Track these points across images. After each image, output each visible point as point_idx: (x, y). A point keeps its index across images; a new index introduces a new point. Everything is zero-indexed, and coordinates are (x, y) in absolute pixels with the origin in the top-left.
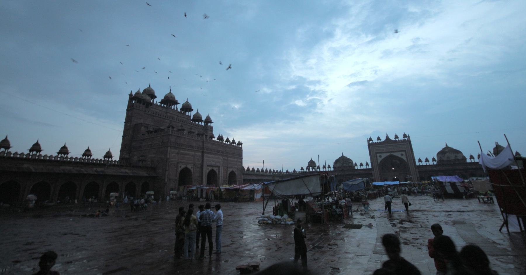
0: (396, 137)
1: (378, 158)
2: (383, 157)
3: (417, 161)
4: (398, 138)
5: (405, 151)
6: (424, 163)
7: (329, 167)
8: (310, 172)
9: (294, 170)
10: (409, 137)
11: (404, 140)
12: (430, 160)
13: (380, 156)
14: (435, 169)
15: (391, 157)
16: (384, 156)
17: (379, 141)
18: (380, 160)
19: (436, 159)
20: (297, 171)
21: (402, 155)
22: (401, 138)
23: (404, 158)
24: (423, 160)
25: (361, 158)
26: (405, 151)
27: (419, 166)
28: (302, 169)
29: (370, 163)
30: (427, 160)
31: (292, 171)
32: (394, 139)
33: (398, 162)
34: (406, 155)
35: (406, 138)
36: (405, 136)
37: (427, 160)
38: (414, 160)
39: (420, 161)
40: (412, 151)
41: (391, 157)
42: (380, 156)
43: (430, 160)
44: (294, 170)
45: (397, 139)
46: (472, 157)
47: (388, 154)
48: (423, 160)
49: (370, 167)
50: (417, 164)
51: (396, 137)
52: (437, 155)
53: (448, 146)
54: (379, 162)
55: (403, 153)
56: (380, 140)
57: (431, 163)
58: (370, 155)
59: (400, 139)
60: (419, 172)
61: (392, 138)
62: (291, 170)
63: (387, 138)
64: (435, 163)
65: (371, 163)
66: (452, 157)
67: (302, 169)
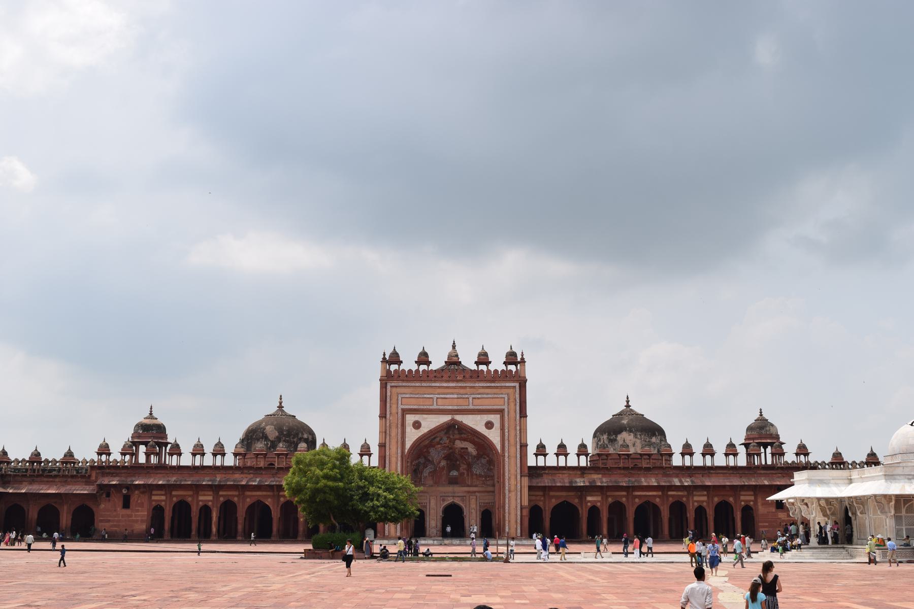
0: (483, 359)
1: (409, 429)
2: (424, 429)
3: (532, 449)
4: (487, 363)
5: (501, 412)
6: (551, 461)
7: (219, 451)
8: (137, 469)
9: (69, 454)
10: (523, 361)
11: (505, 376)
12: (572, 449)
13: (417, 425)
14: (580, 482)
15: (453, 429)
16: (430, 423)
17: (423, 367)
18: (412, 436)
19: (590, 450)
20: (79, 456)
21: (489, 425)
22: (497, 364)
23: (494, 436)
24: (551, 449)
25: (349, 424)
26: (501, 412)
27: (535, 472)
28: (104, 450)
29: (375, 450)
30: (562, 450)
31: (59, 457)
32: (474, 367)
33: (472, 449)
34: (502, 429)
35: (512, 368)
36: (511, 358)
37: (562, 450)
38: (524, 446)
39: (541, 450)
40: (523, 414)
41: (453, 429)
42: (417, 425)
43: (572, 449)
44: (69, 454)
45: (483, 367)
46: (687, 450)
47: (445, 419)
48: (551, 449)
49: (375, 461)
50: (531, 461)
51: (483, 359)
52: (595, 436)
53: (634, 407)
54: (408, 445)
55: (495, 419)
56: (428, 363)
57: (572, 461)
58: (383, 416)
59: (492, 367)
60: (531, 488)
61: (469, 361)
62: (52, 453)
63: (453, 362)
64: (583, 461)
65: (382, 446)
66: (632, 443)
67: (104, 450)
